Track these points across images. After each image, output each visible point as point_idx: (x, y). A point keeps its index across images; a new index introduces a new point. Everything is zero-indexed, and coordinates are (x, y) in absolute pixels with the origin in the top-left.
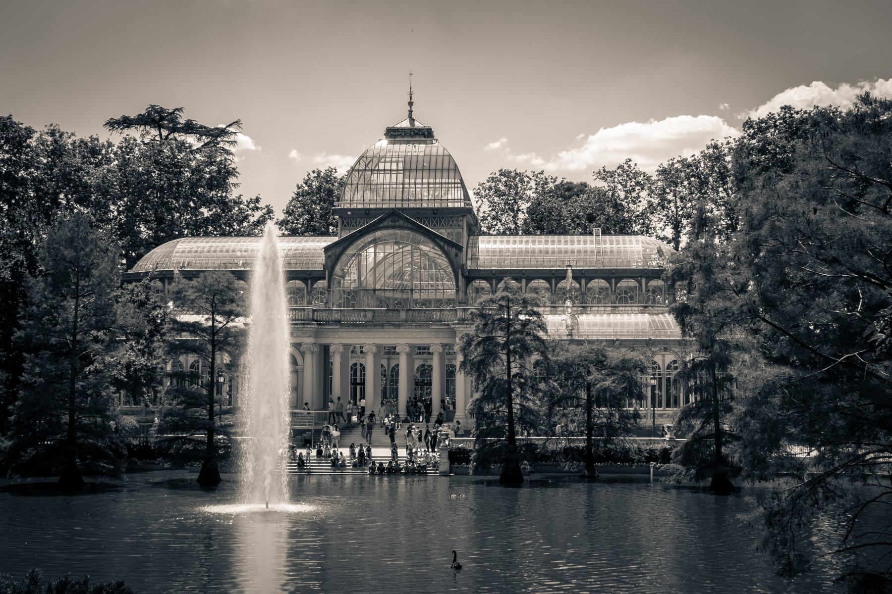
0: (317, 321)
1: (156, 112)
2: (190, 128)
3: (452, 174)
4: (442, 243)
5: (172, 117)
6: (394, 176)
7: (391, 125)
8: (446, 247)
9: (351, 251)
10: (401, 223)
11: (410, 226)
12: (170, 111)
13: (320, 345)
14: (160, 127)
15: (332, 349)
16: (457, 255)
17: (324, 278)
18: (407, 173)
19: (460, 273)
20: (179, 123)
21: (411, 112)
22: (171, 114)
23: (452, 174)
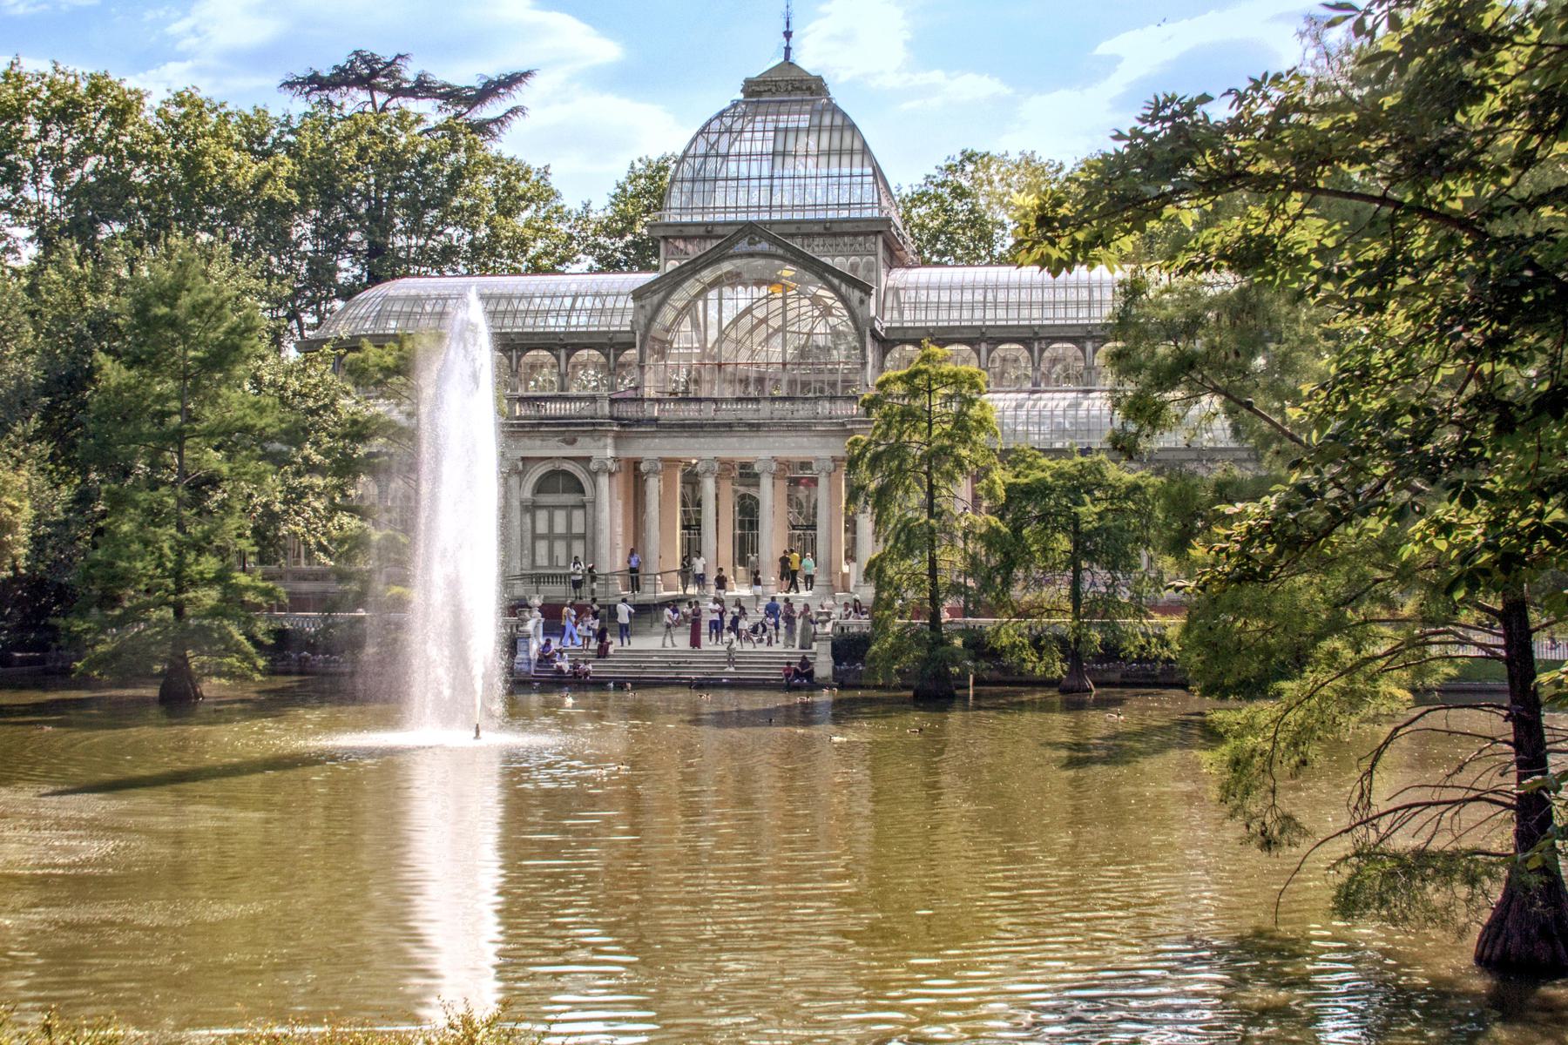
0: (617, 419)
1: (365, 61)
2: (422, 88)
3: (857, 159)
4: (836, 282)
5: (391, 69)
6: (744, 165)
7: (755, 73)
8: (844, 288)
9: (679, 298)
10: (764, 246)
11: (780, 252)
12: (388, 60)
13: (628, 460)
14: (372, 88)
15: (643, 467)
16: (862, 302)
17: (633, 346)
18: (779, 160)
19: (868, 333)
20: (406, 81)
21: (788, 49)
22: (388, 65)
23: (857, 159)
